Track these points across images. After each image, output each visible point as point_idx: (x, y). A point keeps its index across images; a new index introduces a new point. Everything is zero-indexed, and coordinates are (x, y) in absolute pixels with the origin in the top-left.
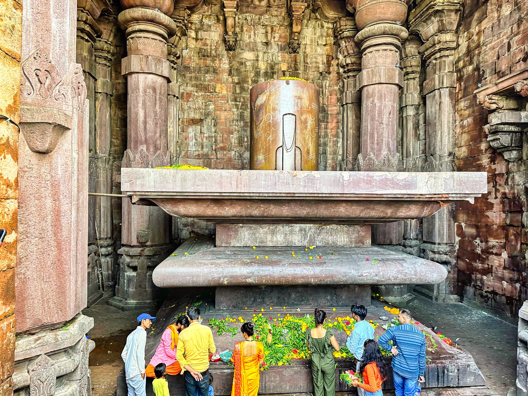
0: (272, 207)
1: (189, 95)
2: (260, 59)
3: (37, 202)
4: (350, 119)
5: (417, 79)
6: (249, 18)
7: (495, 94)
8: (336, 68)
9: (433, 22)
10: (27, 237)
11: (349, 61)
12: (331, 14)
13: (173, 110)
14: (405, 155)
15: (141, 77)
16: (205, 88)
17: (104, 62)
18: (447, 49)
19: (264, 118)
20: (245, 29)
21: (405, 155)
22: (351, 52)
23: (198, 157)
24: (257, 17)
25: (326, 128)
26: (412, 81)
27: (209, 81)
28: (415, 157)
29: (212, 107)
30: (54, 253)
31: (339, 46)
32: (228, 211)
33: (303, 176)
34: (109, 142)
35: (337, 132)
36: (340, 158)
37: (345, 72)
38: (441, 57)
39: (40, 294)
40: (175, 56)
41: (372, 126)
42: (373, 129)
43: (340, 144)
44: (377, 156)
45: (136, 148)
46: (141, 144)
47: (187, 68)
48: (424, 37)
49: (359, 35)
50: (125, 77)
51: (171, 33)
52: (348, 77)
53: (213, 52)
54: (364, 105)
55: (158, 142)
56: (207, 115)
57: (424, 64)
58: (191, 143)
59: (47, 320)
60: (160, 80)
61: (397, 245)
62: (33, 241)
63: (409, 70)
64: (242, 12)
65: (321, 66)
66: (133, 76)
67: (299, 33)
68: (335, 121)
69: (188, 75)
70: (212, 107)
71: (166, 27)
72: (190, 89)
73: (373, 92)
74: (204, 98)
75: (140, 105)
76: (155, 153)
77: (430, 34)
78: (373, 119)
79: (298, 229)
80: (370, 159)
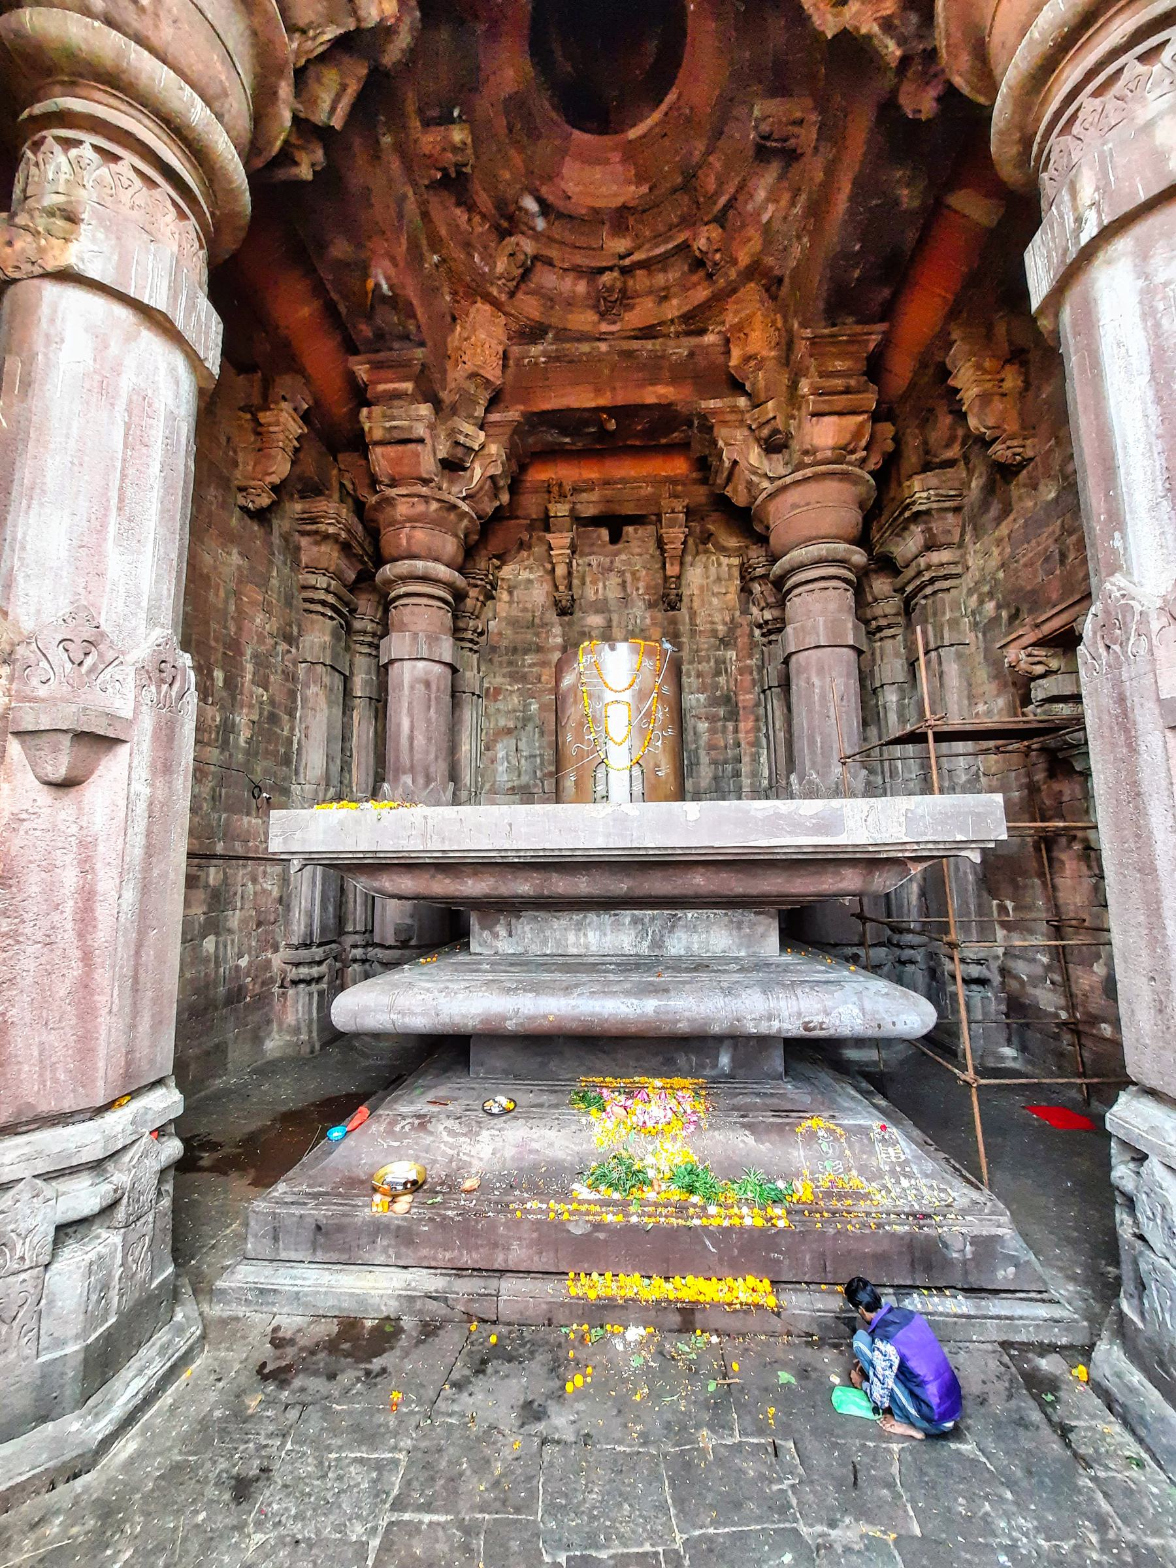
0: (555, 877)
1: (498, 691)
2: (614, 624)
3: (43, 874)
4: (778, 713)
5: (900, 638)
6: (594, 563)
7: (1033, 645)
8: (747, 629)
9: (912, 535)
10: (18, 942)
11: (768, 615)
12: (732, 542)
13: (469, 715)
14: (888, 775)
15: (407, 664)
16: (523, 678)
17: (367, 650)
18: (946, 577)
19: (572, 713)
20: (588, 580)
21: (888, 775)
22: (771, 600)
23: (513, 791)
24: (608, 560)
25: (736, 731)
26: (890, 641)
27: (530, 666)
28: (907, 776)
29: (534, 707)
30: (75, 970)
31: (751, 593)
32: (473, 887)
33: (603, 814)
34: (371, 773)
35: (757, 739)
36: (765, 782)
37: (763, 635)
38: (935, 593)
39: (36, 1053)
40: (475, 631)
41: (810, 721)
42: (811, 728)
43: (763, 759)
44: (823, 775)
45: (397, 779)
46: (404, 773)
47: (494, 649)
48: (900, 562)
49: (777, 569)
50: (386, 667)
51: (459, 596)
52: (770, 642)
53: (537, 621)
54: (794, 687)
55: (432, 770)
56: (526, 720)
57: (908, 609)
58: (500, 769)
59: (47, 1106)
60: (438, 668)
61: (875, 945)
62: (30, 950)
63: (883, 622)
64: (582, 555)
65: (720, 627)
66: (396, 665)
67: (679, 577)
68: (752, 718)
69: (496, 659)
70: (534, 707)
71: (449, 586)
72: (499, 680)
73: (808, 664)
74: (521, 695)
75: (405, 711)
76: (427, 784)
77: (910, 556)
78: (810, 711)
79: (627, 920)
80: (810, 782)
